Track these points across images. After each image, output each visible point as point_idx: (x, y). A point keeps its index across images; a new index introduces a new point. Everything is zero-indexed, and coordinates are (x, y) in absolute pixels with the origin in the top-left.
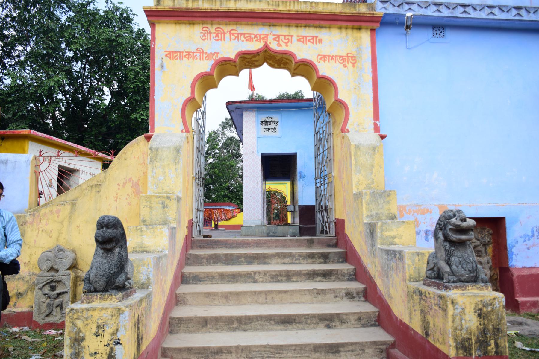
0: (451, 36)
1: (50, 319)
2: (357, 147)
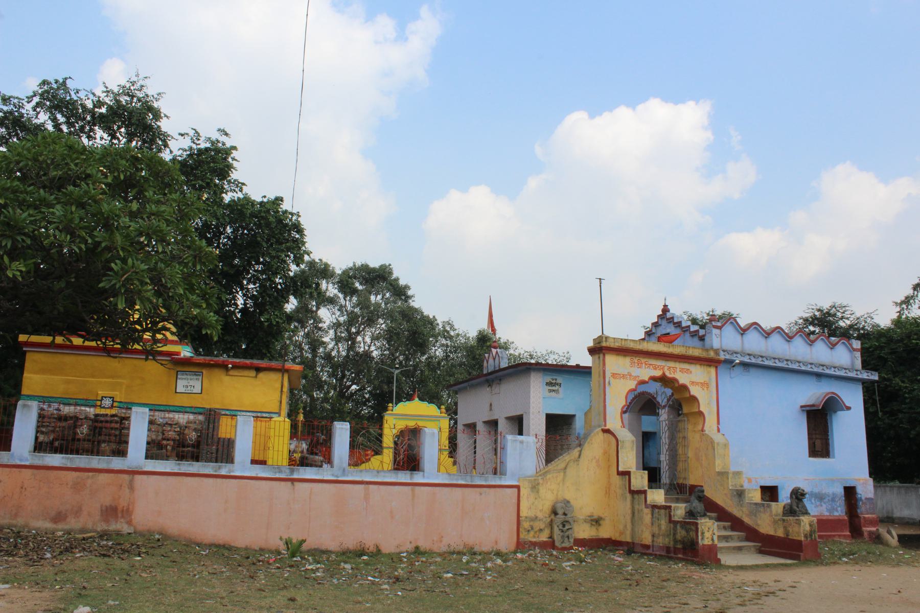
0: (753, 371)
1: (564, 545)
2: (718, 444)
